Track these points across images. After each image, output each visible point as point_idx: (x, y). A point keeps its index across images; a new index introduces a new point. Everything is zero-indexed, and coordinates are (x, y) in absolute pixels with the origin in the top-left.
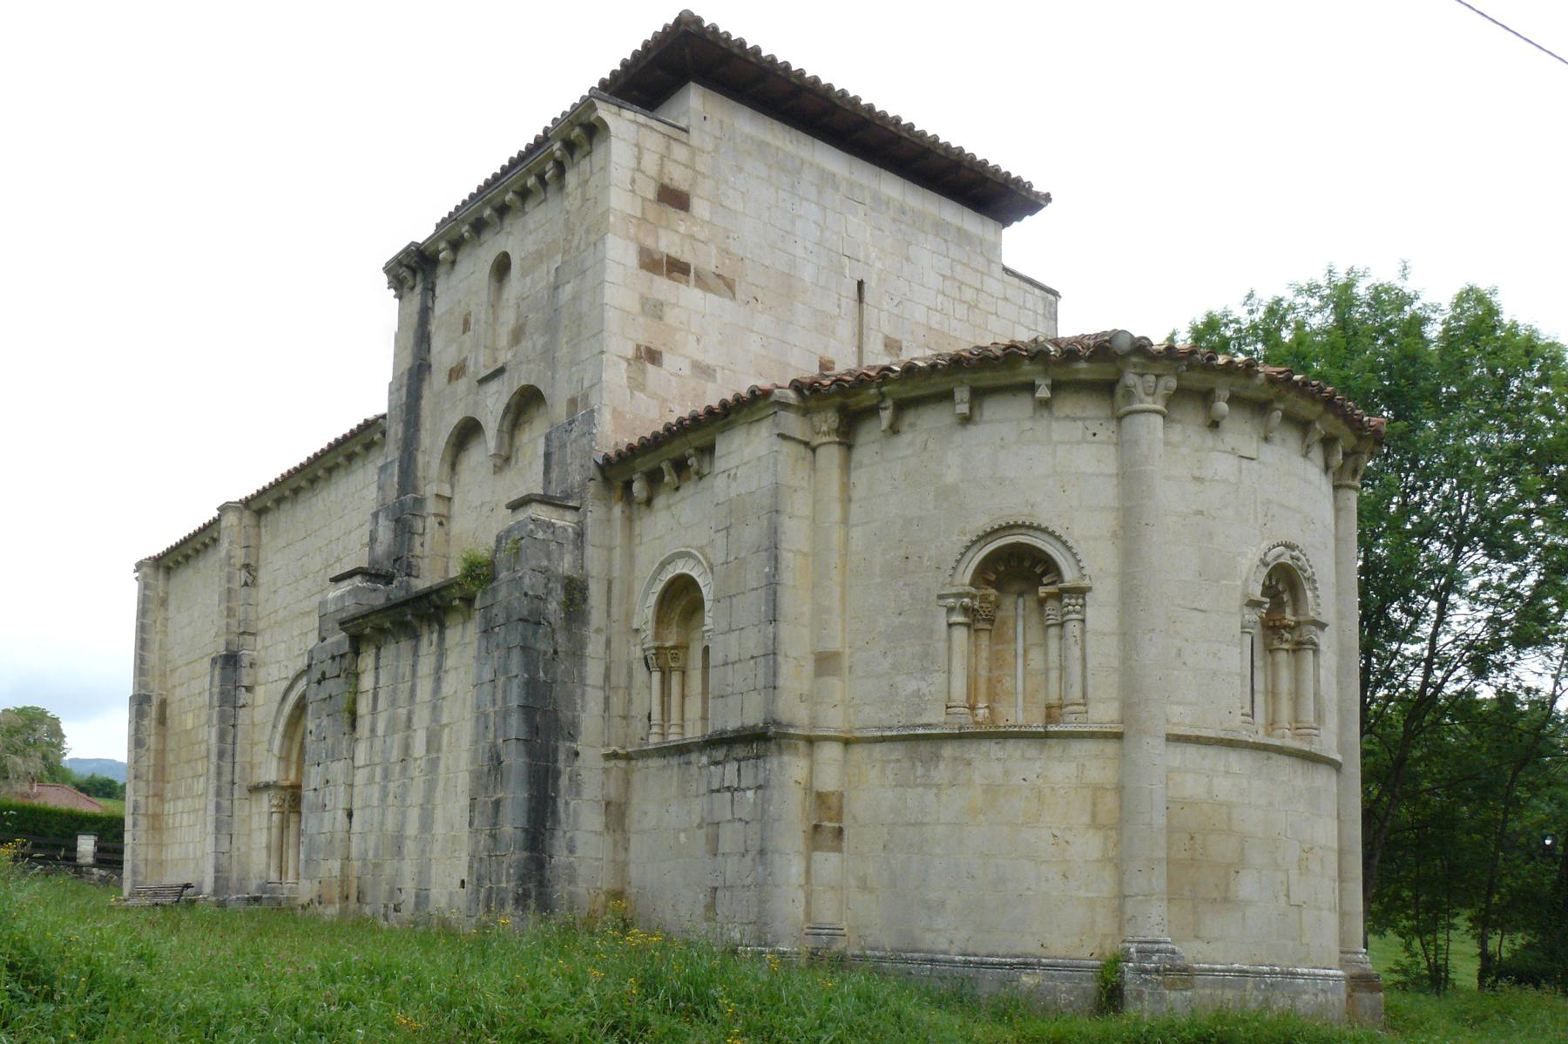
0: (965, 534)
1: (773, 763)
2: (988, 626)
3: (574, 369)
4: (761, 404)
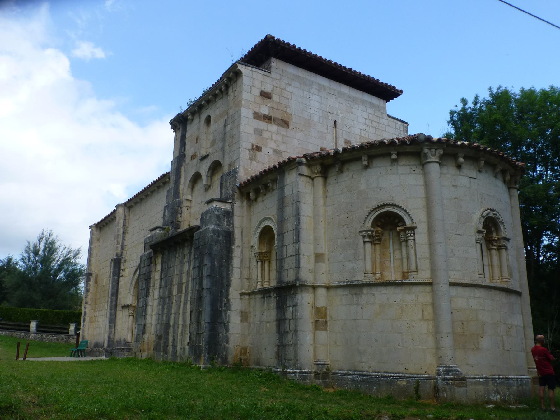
0: (368, 208)
1: (299, 296)
2: (379, 242)
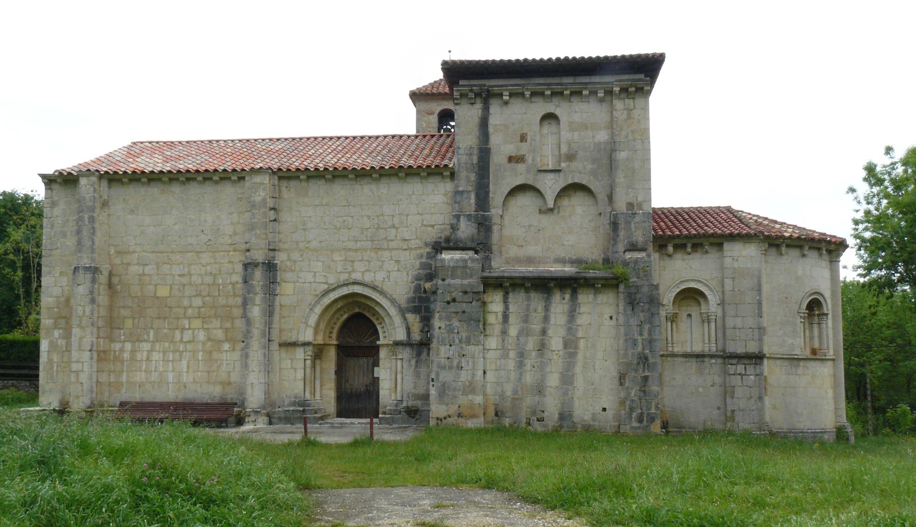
3: (630, 190)
4: (755, 238)
